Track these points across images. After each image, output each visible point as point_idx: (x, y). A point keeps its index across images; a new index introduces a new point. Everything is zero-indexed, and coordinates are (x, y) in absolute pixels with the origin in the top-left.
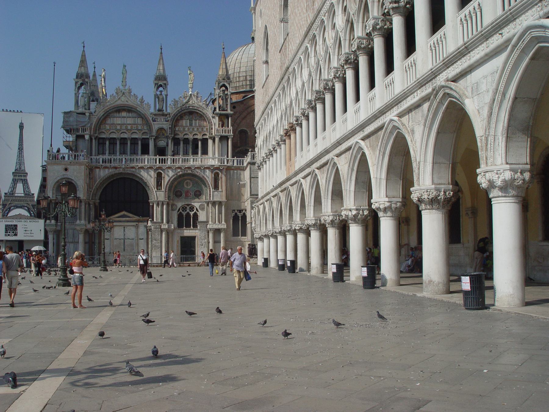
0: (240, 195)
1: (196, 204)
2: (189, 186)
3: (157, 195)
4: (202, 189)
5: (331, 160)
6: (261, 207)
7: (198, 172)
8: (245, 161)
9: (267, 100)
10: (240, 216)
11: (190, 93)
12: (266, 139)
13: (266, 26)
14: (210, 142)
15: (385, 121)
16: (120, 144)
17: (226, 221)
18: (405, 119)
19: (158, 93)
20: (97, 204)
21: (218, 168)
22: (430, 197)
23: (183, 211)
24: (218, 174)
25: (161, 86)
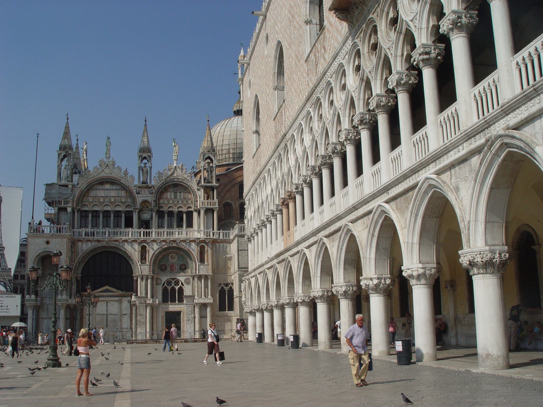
0: (226, 268)
1: (182, 279)
2: (174, 260)
3: (141, 269)
4: (187, 263)
5: (345, 227)
6: (253, 280)
7: (184, 245)
8: (231, 234)
9: (258, 170)
10: (227, 290)
11: (175, 165)
13: (256, 96)
14: (195, 215)
15: (418, 180)
16: (103, 216)
17: (212, 295)
18: (445, 177)
19: (143, 165)
20: (79, 279)
21: (204, 241)
22: (484, 260)
23: (168, 285)
25: (145, 158)
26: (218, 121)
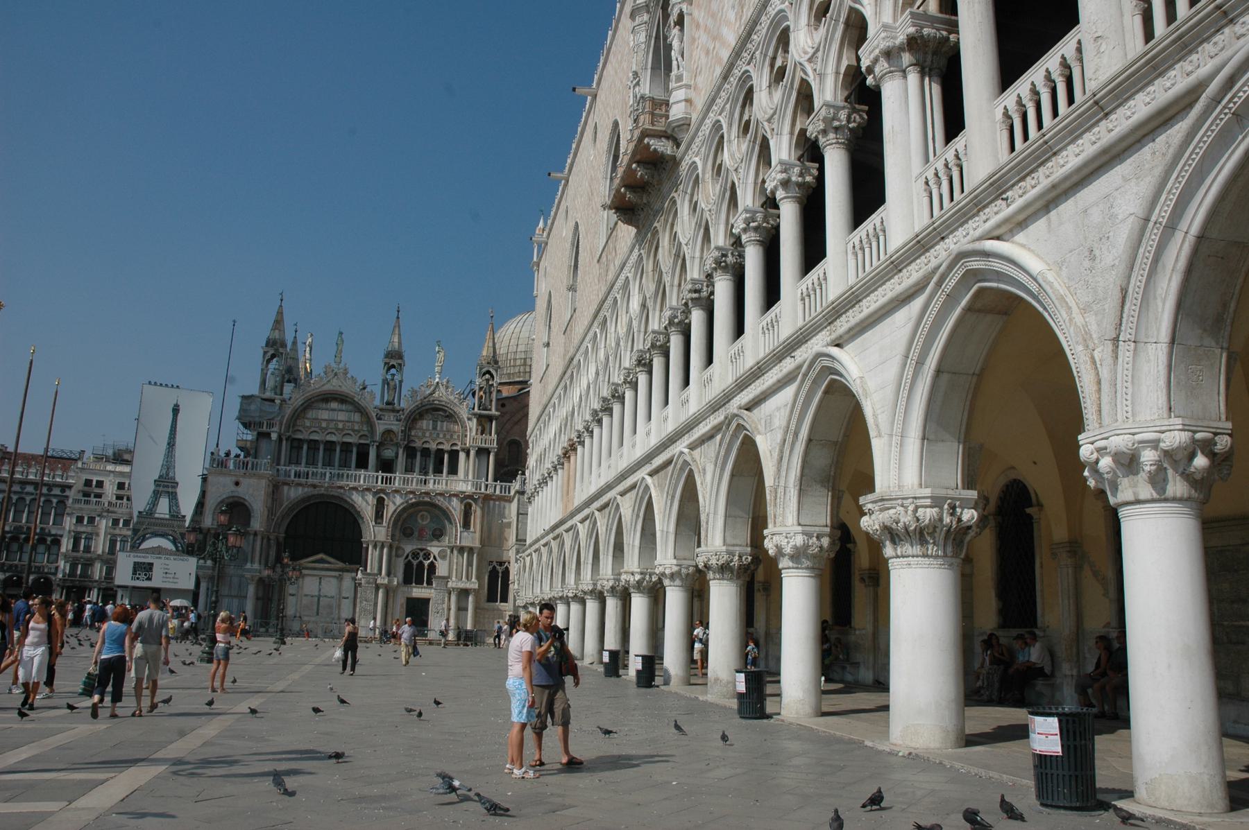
0: (502, 539)
1: (434, 550)
2: (424, 521)
3: (375, 532)
4: (444, 527)
6: (528, 559)
7: (440, 501)
9: (545, 400)
12: (540, 460)
14: (462, 456)
16: (325, 450)
17: (478, 578)
18: (696, 453)
19: (389, 377)
20: (281, 540)
21: (471, 497)
22: (720, 563)
24: (470, 505)
25: (393, 366)
26: (513, 316)
